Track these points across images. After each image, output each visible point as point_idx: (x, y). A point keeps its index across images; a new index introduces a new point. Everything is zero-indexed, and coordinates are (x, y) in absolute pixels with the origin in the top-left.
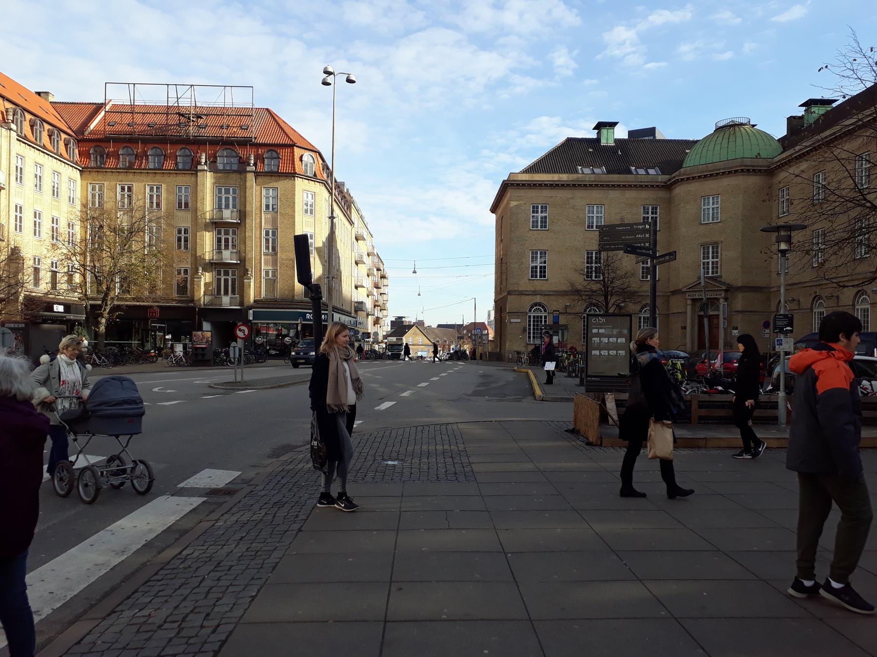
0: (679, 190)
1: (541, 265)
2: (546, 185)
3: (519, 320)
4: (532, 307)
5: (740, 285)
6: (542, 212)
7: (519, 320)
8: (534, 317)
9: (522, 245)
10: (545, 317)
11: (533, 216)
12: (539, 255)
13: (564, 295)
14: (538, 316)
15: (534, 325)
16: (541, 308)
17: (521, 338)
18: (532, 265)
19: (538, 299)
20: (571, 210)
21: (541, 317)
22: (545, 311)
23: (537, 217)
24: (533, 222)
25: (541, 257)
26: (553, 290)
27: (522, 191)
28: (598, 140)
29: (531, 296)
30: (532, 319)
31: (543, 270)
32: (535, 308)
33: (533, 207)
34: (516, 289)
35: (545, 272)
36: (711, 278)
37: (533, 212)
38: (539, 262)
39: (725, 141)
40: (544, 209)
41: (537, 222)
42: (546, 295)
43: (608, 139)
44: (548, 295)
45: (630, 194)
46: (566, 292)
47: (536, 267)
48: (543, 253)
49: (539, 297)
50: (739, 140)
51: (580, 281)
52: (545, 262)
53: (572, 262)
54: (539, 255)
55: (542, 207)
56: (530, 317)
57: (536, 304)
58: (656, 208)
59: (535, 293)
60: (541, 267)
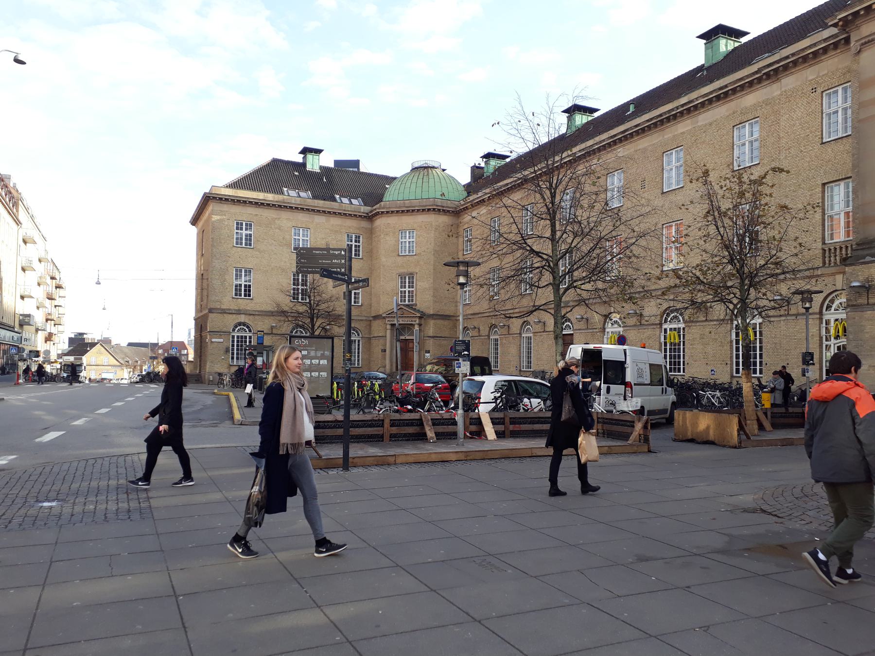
0: (380, 222)
1: (246, 283)
2: (251, 202)
3: (221, 340)
4: (236, 327)
5: (432, 313)
6: (246, 229)
7: (221, 340)
8: (238, 337)
9: (225, 261)
10: (250, 337)
11: (237, 233)
12: (243, 274)
13: (270, 316)
14: (242, 337)
15: (238, 346)
16: (245, 328)
17: (223, 359)
18: (235, 282)
19: (242, 318)
20: (277, 230)
21: (246, 337)
22: (250, 331)
23: (242, 234)
24: (237, 239)
25: (245, 276)
26: (259, 309)
27: (225, 206)
28: (304, 165)
29: (234, 316)
30: (236, 339)
31: (248, 289)
32: (239, 327)
33: (237, 224)
34: (219, 307)
35: (250, 291)
36: (407, 306)
37: (237, 229)
38: (243, 280)
39: (420, 181)
40: (249, 226)
41: (241, 239)
42: (251, 315)
43: (314, 164)
44: (253, 315)
45: (335, 221)
46: (272, 312)
47: (241, 285)
48: (248, 272)
49: (243, 316)
50: (431, 181)
51: (286, 302)
52: (250, 281)
53: (278, 282)
54: (243, 274)
55: (246, 224)
56: (233, 337)
57: (240, 324)
58: (359, 237)
59: (239, 312)
60: (245, 286)
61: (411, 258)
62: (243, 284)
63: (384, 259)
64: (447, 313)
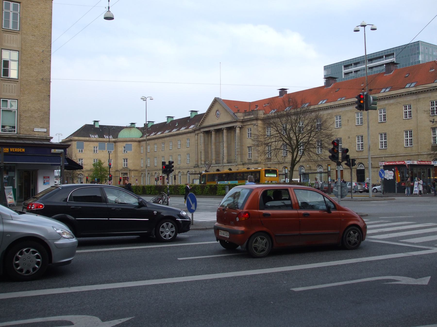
5: (132, 169)
28: (94, 125)
36: (126, 167)
43: (97, 126)
61: (127, 154)
62: (81, 163)
63: (119, 154)
64: (137, 169)
